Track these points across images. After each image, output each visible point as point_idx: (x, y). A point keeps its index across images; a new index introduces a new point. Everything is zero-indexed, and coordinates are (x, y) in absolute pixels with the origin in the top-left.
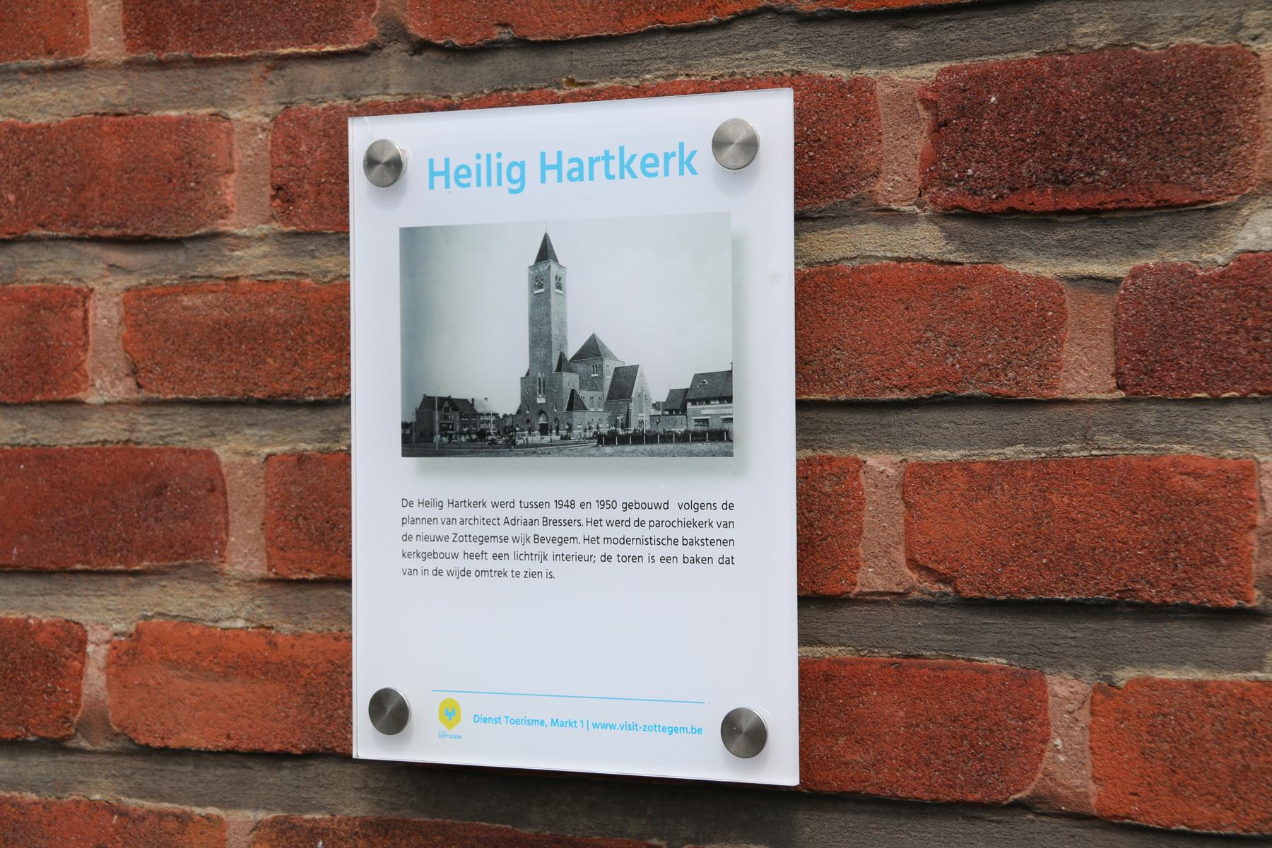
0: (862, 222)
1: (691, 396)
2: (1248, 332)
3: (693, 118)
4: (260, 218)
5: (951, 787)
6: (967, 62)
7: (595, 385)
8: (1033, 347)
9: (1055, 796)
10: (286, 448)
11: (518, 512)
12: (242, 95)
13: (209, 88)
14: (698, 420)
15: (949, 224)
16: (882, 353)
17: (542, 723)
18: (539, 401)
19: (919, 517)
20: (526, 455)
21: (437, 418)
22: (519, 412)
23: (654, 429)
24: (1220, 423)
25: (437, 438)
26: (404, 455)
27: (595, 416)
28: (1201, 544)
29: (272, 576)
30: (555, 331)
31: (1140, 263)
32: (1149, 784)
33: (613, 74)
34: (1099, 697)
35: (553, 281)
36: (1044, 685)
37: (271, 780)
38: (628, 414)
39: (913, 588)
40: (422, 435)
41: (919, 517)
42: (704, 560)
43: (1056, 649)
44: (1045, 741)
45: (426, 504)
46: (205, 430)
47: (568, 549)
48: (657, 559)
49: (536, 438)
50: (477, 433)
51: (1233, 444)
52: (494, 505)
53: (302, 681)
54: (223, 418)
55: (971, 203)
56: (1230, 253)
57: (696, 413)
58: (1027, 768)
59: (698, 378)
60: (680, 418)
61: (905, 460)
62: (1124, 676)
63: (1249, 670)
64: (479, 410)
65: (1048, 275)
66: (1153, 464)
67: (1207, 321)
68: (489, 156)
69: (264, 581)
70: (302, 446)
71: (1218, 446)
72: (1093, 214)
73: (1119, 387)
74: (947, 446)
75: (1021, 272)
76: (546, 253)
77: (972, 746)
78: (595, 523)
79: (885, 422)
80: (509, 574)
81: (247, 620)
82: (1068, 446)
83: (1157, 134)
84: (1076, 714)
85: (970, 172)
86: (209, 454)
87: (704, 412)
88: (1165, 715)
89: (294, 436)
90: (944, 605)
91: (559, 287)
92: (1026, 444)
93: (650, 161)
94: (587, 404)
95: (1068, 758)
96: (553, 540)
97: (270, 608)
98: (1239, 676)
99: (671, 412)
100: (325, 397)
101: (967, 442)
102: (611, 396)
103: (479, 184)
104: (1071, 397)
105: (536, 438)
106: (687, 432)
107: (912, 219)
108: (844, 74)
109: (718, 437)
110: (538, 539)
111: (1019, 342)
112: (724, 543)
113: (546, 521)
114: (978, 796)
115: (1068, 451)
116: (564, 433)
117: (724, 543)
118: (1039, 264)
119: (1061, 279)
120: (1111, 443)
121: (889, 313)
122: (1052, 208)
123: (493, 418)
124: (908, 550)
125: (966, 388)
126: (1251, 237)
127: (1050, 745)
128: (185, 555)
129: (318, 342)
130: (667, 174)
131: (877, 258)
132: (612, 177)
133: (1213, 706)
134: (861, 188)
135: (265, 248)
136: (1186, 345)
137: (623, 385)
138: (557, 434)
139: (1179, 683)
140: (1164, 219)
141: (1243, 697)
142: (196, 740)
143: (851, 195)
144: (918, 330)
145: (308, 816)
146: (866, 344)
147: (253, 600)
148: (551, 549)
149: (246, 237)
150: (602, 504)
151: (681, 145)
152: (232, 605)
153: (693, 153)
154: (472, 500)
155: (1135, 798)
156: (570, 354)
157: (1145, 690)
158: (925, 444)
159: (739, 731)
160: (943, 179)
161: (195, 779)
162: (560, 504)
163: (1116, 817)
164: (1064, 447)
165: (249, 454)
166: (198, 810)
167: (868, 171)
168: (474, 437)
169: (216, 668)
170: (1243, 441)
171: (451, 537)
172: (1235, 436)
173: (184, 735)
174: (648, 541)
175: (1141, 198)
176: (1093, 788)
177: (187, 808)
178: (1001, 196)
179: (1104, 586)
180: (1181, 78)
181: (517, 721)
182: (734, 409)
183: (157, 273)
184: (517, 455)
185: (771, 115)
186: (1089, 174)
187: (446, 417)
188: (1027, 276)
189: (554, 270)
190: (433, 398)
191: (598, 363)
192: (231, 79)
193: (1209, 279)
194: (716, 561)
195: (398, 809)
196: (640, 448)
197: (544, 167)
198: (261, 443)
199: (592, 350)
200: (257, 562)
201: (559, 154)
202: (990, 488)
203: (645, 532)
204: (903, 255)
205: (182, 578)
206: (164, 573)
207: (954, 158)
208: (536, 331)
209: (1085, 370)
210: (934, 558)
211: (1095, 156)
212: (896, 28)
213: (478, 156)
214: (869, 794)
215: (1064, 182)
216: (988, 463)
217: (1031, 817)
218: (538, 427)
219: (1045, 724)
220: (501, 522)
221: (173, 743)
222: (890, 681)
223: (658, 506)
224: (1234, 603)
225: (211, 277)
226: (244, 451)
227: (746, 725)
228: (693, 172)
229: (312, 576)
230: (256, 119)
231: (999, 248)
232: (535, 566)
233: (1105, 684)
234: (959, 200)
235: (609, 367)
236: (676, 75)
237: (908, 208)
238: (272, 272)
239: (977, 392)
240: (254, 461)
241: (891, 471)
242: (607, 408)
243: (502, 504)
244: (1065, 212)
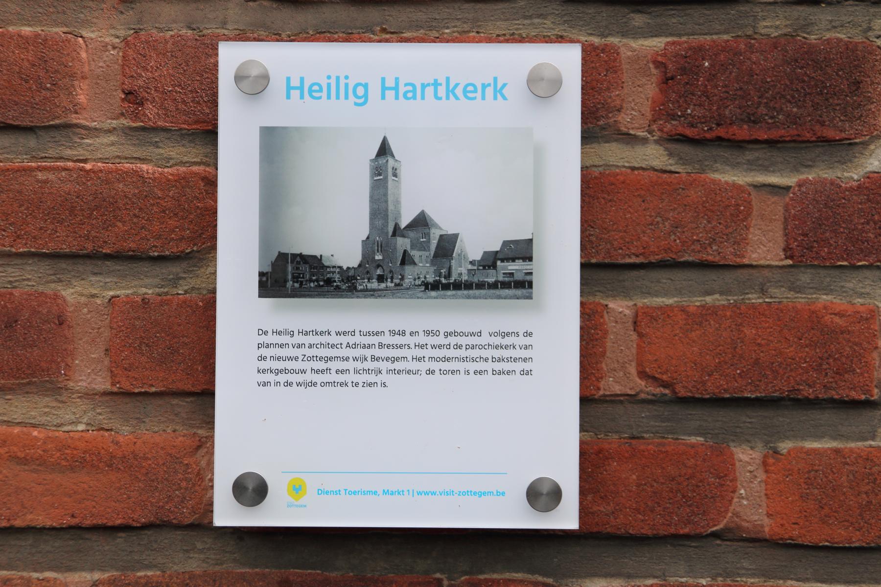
0: (606, 142)
1: (500, 256)
2: (875, 223)
3: (508, 62)
4: (109, 115)
5: (669, 525)
6: (684, 39)
7: (424, 247)
8: (730, 230)
9: (739, 528)
10: (130, 292)
11: (358, 339)
12: (95, 20)
13: (64, 13)
14: (507, 272)
15: (670, 146)
16: (625, 231)
17: (375, 493)
18: (377, 258)
19: (649, 343)
20: (365, 297)
21: (290, 269)
22: (360, 266)
23: (471, 279)
24: (852, 282)
26: (260, 296)
27: (423, 268)
28: (844, 359)
29: (115, 389)
30: (391, 207)
31: (803, 177)
32: (806, 516)
33: (418, 27)
34: (771, 461)
35: (390, 171)
36: (732, 454)
37: (107, 548)
39: (641, 391)
40: (276, 281)
41: (649, 343)
42: (508, 373)
43: (738, 430)
44: (734, 492)
45: (279, 333)
46: (53, 277)
47: (398, 366)
48: (472, 372)
49: (374, 285)
50: (324, 281)
51: (861, 295)
52: (338, 333)
53: (144, 471)
54: (70, 268)
55: (689, 132)
56: (862, 173)
57: (505, 268)
58: (722, 510)
59: (506, 243)
61: (635, 305)
62: (785, 446)
63: (866, 440)
64: (326, 264)
65: (741, 183)
66: (812, 308)
67: (849, 216)
68: (338, 78)
69: (105, 394)
70: (144, 290)
71: (851, 296)
72: (771, 143)
73: (786, 258)
74: (665, 296)
75: (723, 180)
76: (384, 150)
77: (684, 497)
78: (421, 347)
79: (621, 278)
80: (350, 384)
81: (88, 424)
82: (750, 296)
83: (818, 94)
84: (755, 473)
85: (689, 111)
86: (56, 296)
87: (510, 268)
88: (817, 471)
89: (136, 283)
90: (662, 402)
92: (721, 293)
93: (470, 88)
94: (416, 260)
95: (751, 501)
96: (387, 359)
97: (110, 415)
98: (860, 444)
99: (484, 268)
100: (167, 253)
101: (679, 292)
102: (436, 255)
103: (329, 97)
104: (755, 263)
105: (374, 285)
106: (496, 282)
107: (644, 141)
108: (596, 40)
109: (523, 285)
110: (374, 358)
111: (721, 226)
112: (525, 360)
113: (381, 346)
114: (686, 530)
115: (749, 299)
116: (397, 281)
117: (525, 360)
118: (734, 176)
119: (750, 185)
120: (780, 294)
121: (631, 204)
122: (747, 138)
123: (338, 270)
124: (640, 364)
125: (683, 256)
126: (876, 163)
127: (737, 494)
128: (33, 375)
129: (164, 212)
130: (483, 98)
131: (617, 166)
132: (440, 99)
133: (848, 464)
134: (608, 118)
135: (113, 138)
136: (834, 231)
137: (446, 247)
138: (392, 282)
139: (826, 450)
140: (820, 149)
141: (867, 458)
142: (41, 519)
143: (601, 123)
144: (651, 216)
145: (140, 574)
146: (613, 225)
147: (94, 409)
148: (384, 366)
149: (96, 129)
150: (427, 333)
151: (495, 79)
152: (74, 413)
153: (504, 85)
154: (319, 330)
155: (796, 526)
156: (403, 224)
157: (803, 455)
158: (649, 293)
159: (542, 494)
160: (669, 115)
161: (34, 550)
162: (393, 333)
163: (781, 539)
164: (747, 296)
165: (93, 296)
166: (35, 575)
167: (615, 107)
168: (322, 283)
169: (64, 463)
170: (868, 294)
171: (301, 358)
172: (863, 290)
173: (30, 517)
174: (464, 359)
175: (808, 135)
176: (766, 521)
177: (25, 574)
178: (711, 129)
179: (778, 387)
180: (833, 59)
181: (355, 493)
182: (534, 266)
183: (8, 153)
184: (358, 297)
185: (567, 60)
186: (772, 118)
187: (298, 268)
188: (727, 183)
190: (287, 254)
191: (426, 231)
192: (85, 7)
193: (851, 189)
194: (518, 372)
195: (222, 564)
196: (459, 292)
197: (384, 89)
198: (105, 287)
199: (421, 222)
200: (99, 379)
201: (397, 79)
202: (701, 323)
203: (462, 353)
204: (637, 165)
205: (27, 393)
206: (10, 389)
207: (678, 101)
208: (376, 206)
209: (765, 246)
210: (659, 370)
211: (776, 106)
212: (633, 12)
213: (329, 77)
214: (608, 533)
215: (754, 122)
216: (698, 307)
217: (718, 542)
218: (376, 277)
219: (734, 480)
220: (344, 346)
221: (18, 523)
222: (626, 455)
223: (473, 334)
224: (863, 397)
225: (61, 158)
226: (87, 295)
227: (545, 489)
228: (505, 98)
229: (153, 389)
230: (107, 40)
231: (707, 163)
232: (372, 378)
233: (771, 452)
234: (680, 130)
235: (435, 235)
236: (469, 32)
237: (641, 134)
238: (118, 157)
239: (691, 259)
240: (99, 301)
241: (627, 312)
242: (432, 264)
243: (345, 333)
244: (756, 142)
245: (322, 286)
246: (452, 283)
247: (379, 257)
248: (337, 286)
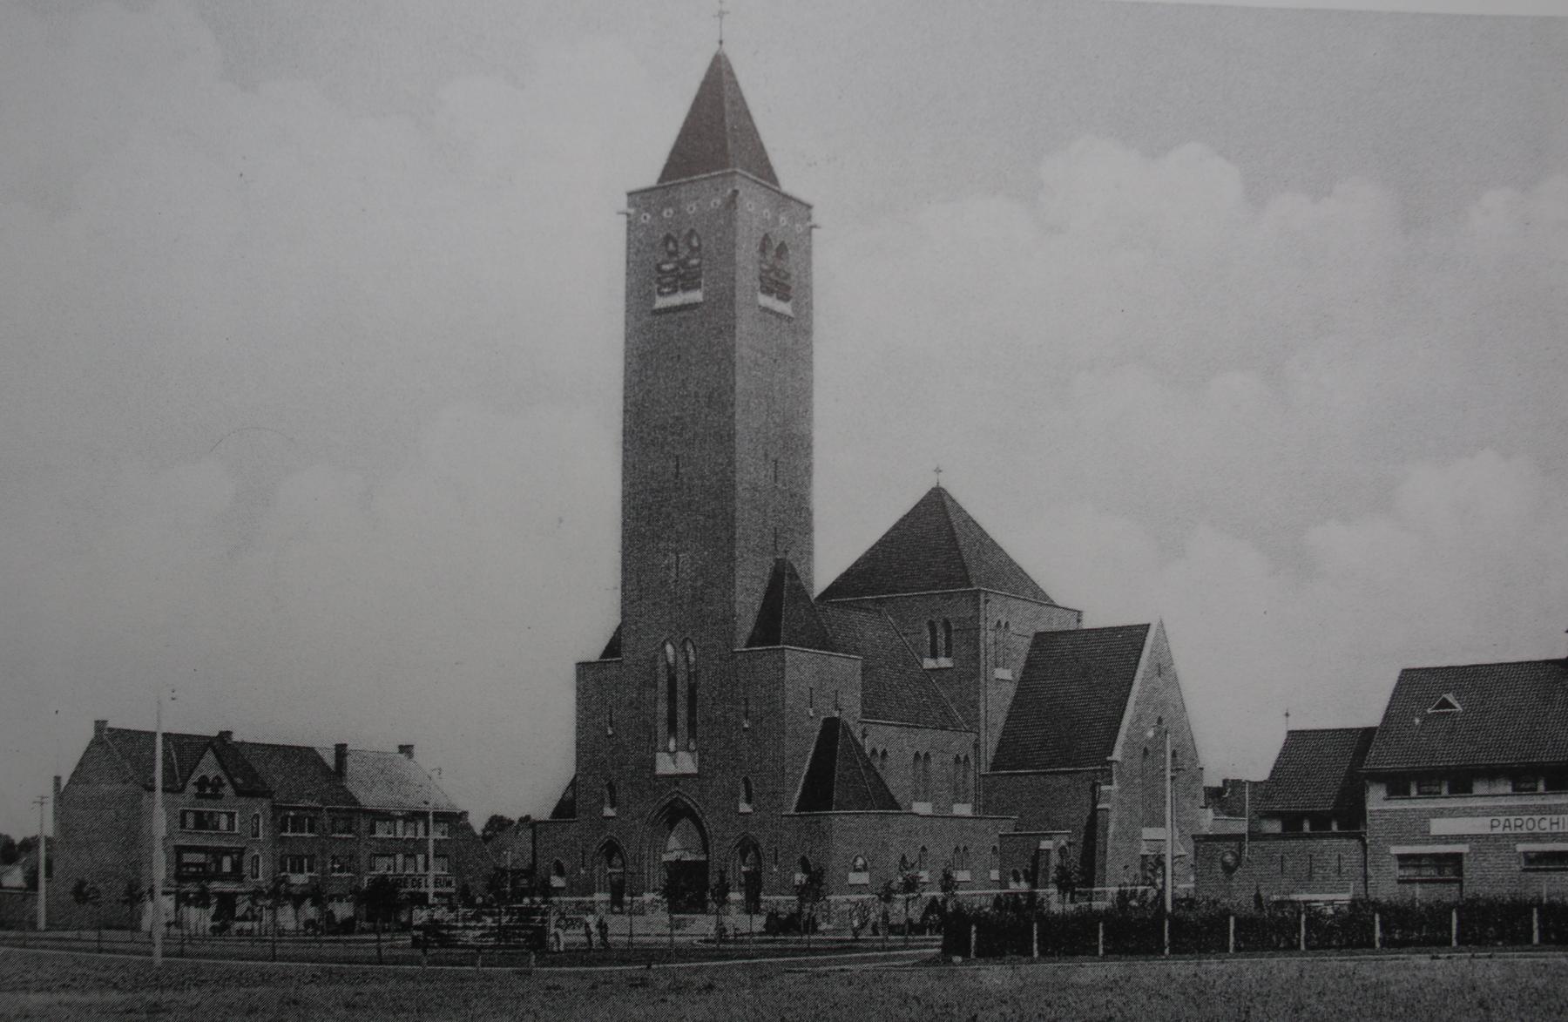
7: (944, 705)
18: (664, 765)
21: (160, 822)
22: (565, 809)
25: (158, 910)
30: (750, 471)
38: (1092, 829)
40: (81, 893)
49: (650, 922)
50: (359, 897)
59: (1416, 685)
60: (1335, 849)
64: (370, 798)
76: (716, 135)
87: (1439, 826)
91: (777, 285)
94: (897, 783)
99: (1291, 824)
102: (1010, 755)
105: (650, 922)
116: (784, 902)
123: (436, 834)
168: (343, 910)
189: (753, 206)
190: (152, 735)
218: (659, 877)
235: (1008, 631)
245: (348, 926)
246: (1106, 915)
247: (675, 762)
248: (433, 927)
